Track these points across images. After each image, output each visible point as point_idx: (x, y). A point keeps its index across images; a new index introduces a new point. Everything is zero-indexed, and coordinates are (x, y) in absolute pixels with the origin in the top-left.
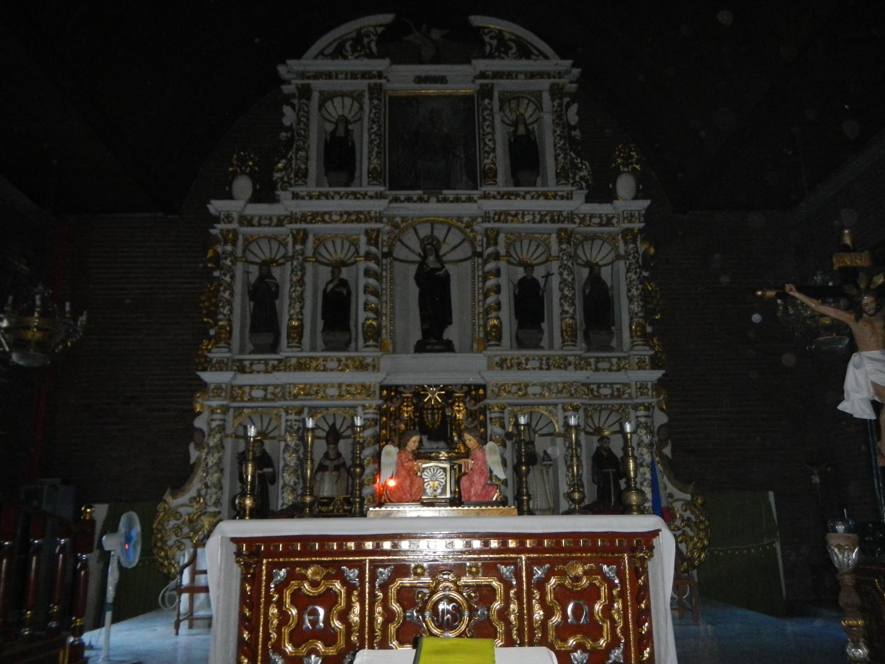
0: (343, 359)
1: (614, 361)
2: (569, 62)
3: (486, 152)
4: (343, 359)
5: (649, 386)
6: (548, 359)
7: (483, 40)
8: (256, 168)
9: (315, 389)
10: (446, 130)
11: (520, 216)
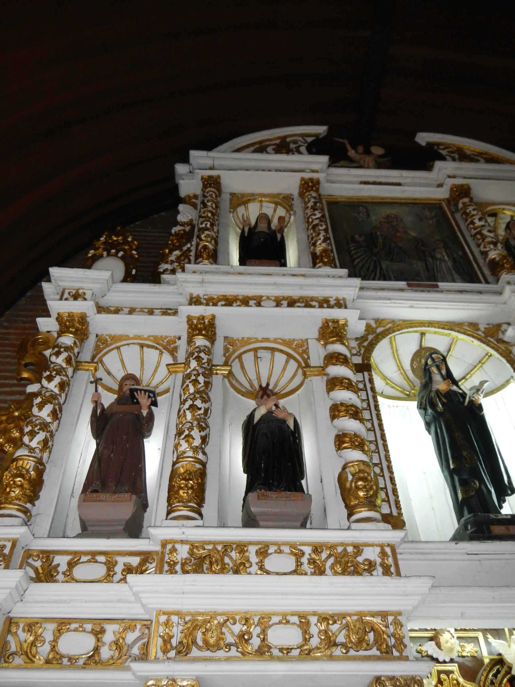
0: (307, 550)
3: (490, 243)
4: (307, 550)
8: (134, 252)
9: (237, 628)
10: (414, 234)
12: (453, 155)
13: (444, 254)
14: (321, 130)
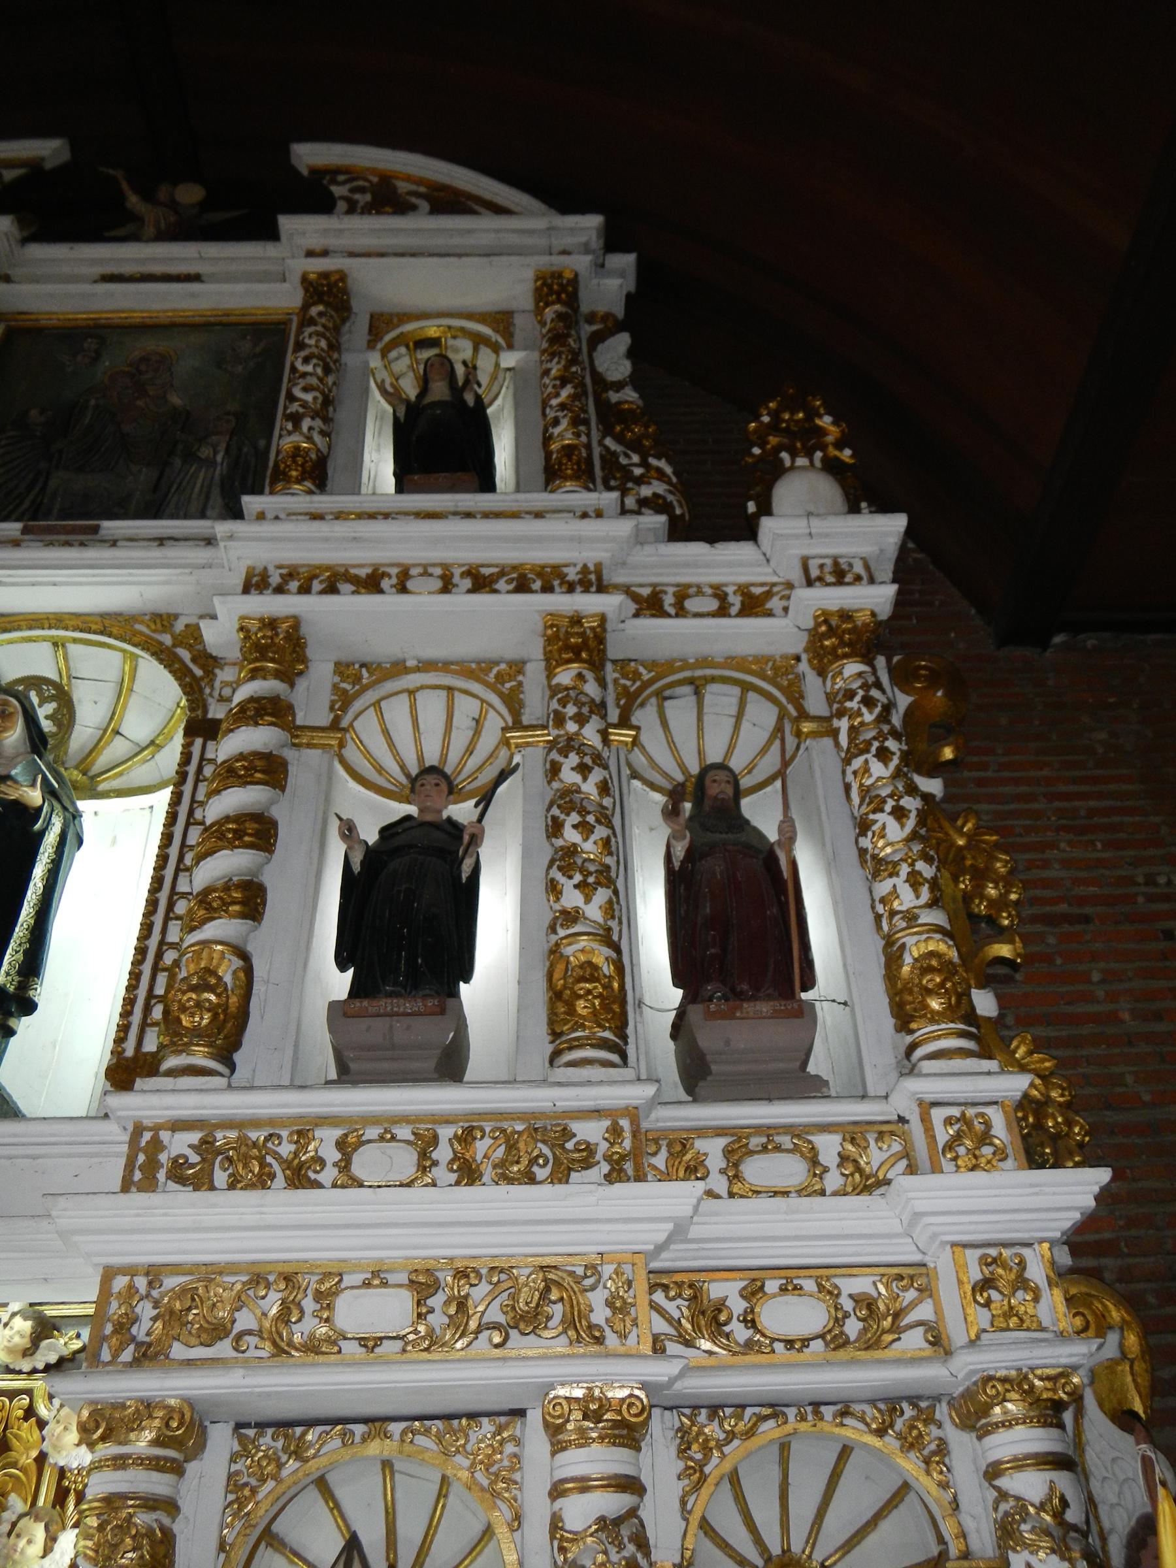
1: (829, 1146)
2: (593, 222)
5: (1037, 1272)
6: (467, 1137)
7: (331, 194)
10: (176, 400)
11: (385, 584)
12: (357, 196)
13: (222, 448)
14: (48, 150)
